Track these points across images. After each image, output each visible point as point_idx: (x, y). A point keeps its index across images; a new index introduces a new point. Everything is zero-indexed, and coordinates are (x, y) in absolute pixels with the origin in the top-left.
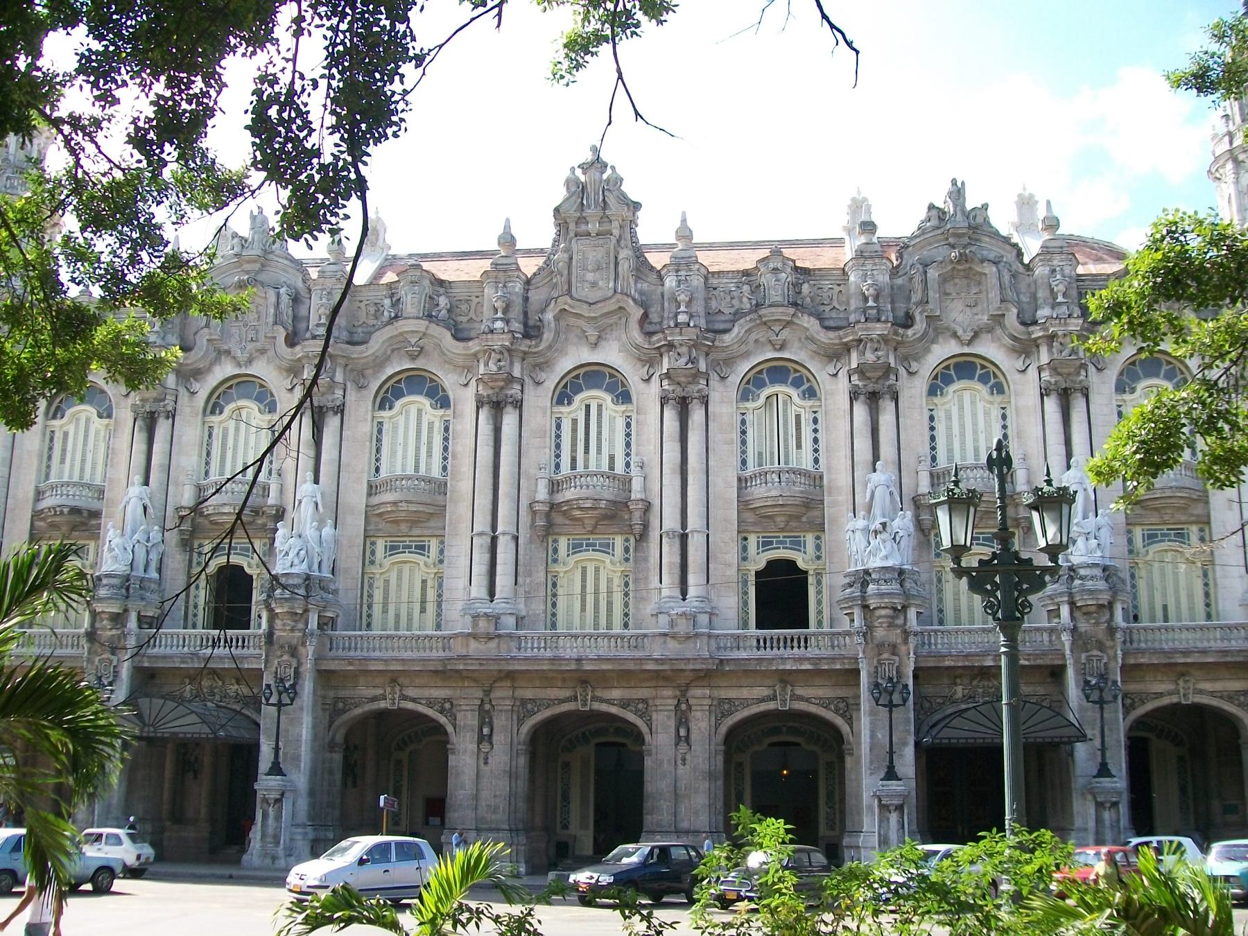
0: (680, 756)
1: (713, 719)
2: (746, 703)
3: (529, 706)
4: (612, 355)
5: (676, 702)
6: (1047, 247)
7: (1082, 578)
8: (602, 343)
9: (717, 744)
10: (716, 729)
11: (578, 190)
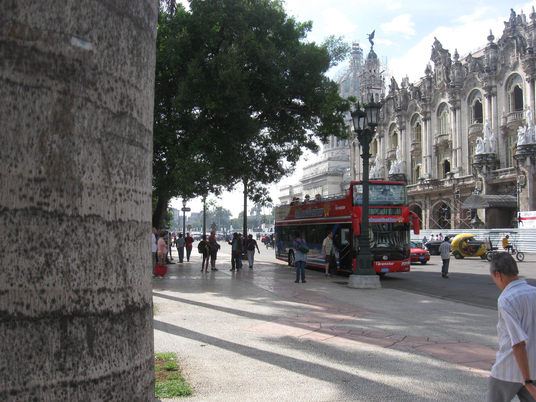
11: (434, 52)
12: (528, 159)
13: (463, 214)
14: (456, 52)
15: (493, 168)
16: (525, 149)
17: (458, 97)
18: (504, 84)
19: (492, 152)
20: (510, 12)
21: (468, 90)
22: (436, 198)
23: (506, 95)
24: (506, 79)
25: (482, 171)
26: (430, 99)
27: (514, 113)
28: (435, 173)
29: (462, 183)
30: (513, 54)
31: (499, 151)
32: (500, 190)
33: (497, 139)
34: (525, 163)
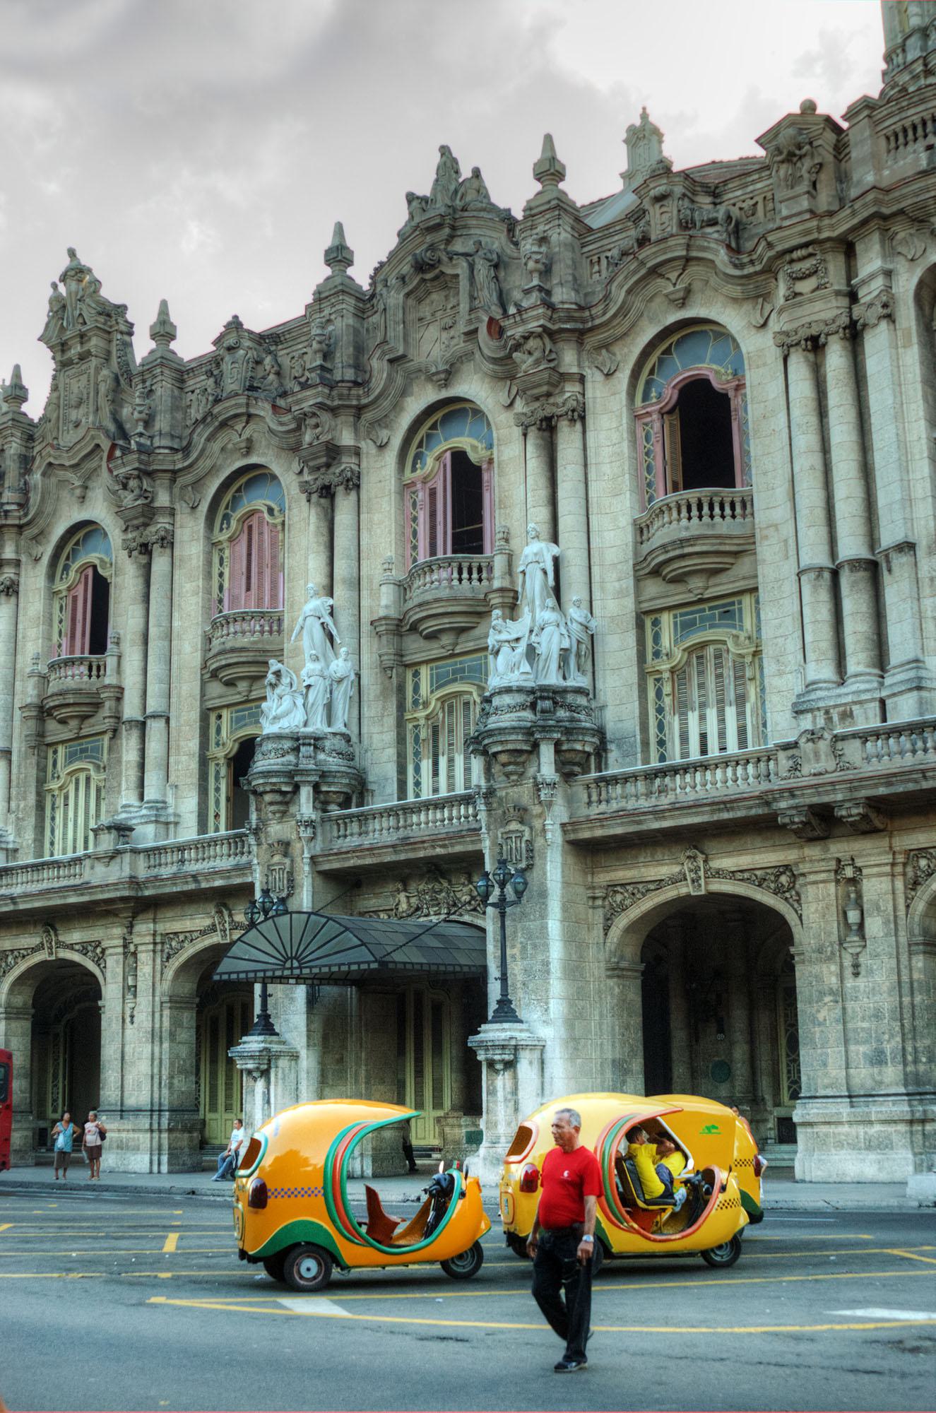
0: (128, 1013)
1: (158, 961)
2: (189, 936)
3: (10, 959)
4: (99, 510)
5: (120, 942)
6: (531, 209)
7: (570, 708)
8: (90, 494)
9: (162, 995)
10: (162, 974)
11: (59, 308)
12: (547, 753)
13: (167, 1012)
14: (164, 308)
15: (341, 800)
16: (533, 706)
17: (163, 499)
18: (396, 442)
19: (339, 727)
20: (436, 158)
21: (213, 470)
22: (28, 940)
23: (405, 488)
24: (405, 420)
25: (293, 809)
26: (23, 505)
27: (449, 562)
28: (19, 832)
29: (174, 869)
30: (449, 321)
31: (365, 730)
32: (370, 902)
33: (358, 676)
34: (531, 771)
